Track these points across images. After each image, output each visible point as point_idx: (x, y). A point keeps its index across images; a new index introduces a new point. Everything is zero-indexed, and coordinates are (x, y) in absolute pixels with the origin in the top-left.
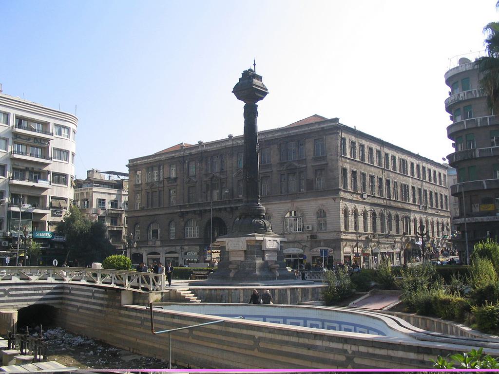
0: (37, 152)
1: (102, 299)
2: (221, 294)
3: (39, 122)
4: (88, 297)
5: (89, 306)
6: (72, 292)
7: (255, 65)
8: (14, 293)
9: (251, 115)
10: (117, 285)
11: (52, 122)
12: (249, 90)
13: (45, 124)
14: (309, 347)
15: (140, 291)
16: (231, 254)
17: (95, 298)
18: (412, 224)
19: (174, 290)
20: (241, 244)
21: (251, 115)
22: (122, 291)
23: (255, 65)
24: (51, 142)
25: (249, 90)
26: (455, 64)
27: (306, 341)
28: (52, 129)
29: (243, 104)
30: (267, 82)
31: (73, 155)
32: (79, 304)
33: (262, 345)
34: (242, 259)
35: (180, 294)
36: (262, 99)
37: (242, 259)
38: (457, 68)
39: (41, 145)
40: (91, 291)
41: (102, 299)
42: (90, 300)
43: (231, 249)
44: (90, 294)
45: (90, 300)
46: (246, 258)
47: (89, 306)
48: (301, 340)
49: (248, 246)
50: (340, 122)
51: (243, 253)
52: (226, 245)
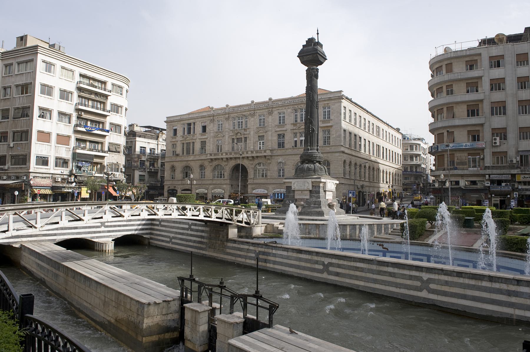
0: (97, 105)
1: (202, 231)
2: (310, 228)
3: (99, 81)
4: (183, 229)
5: (184, 237)
6: (162, 223)
7: (318, 34)
8: (109, 224)
9: (312, 77)
10: (227, 219)
11: (110, 82)
12: (312, 55)
13: (104, 83)
14: (509, 293)
15: (243, 225)
16: (296, 192)
17: (192, 230)
18: (381, 174)
19: (271, 224)
20: (307, 185)
21: (312, 77)
22: (229, 225)
23: (318, 34)
24: (109, 97)
25: (312, 55)
26: (441, 51)
27: (504, 286)
28: (109, 87)
29: (306, 68)
30: (326, 50)
31: (126, 109)
32: (172, 235)
33: (432, 286)
34: (308, 197)
35: (278, 227)
36: (321, 63)
37: (308, 197)
38: (443, 54)
39: (101, 98)
40: (188, 224)
41: (202, 231)
42: (185, 232)
43: (297, 188)
44: (187, 226)
45: (185, 232)
46: (311, 196)
47: (184, 237)
48: (497, 285)
49: (313, 186)
50: (342, 93)
51: (308, 192)
52: (292, 185)
